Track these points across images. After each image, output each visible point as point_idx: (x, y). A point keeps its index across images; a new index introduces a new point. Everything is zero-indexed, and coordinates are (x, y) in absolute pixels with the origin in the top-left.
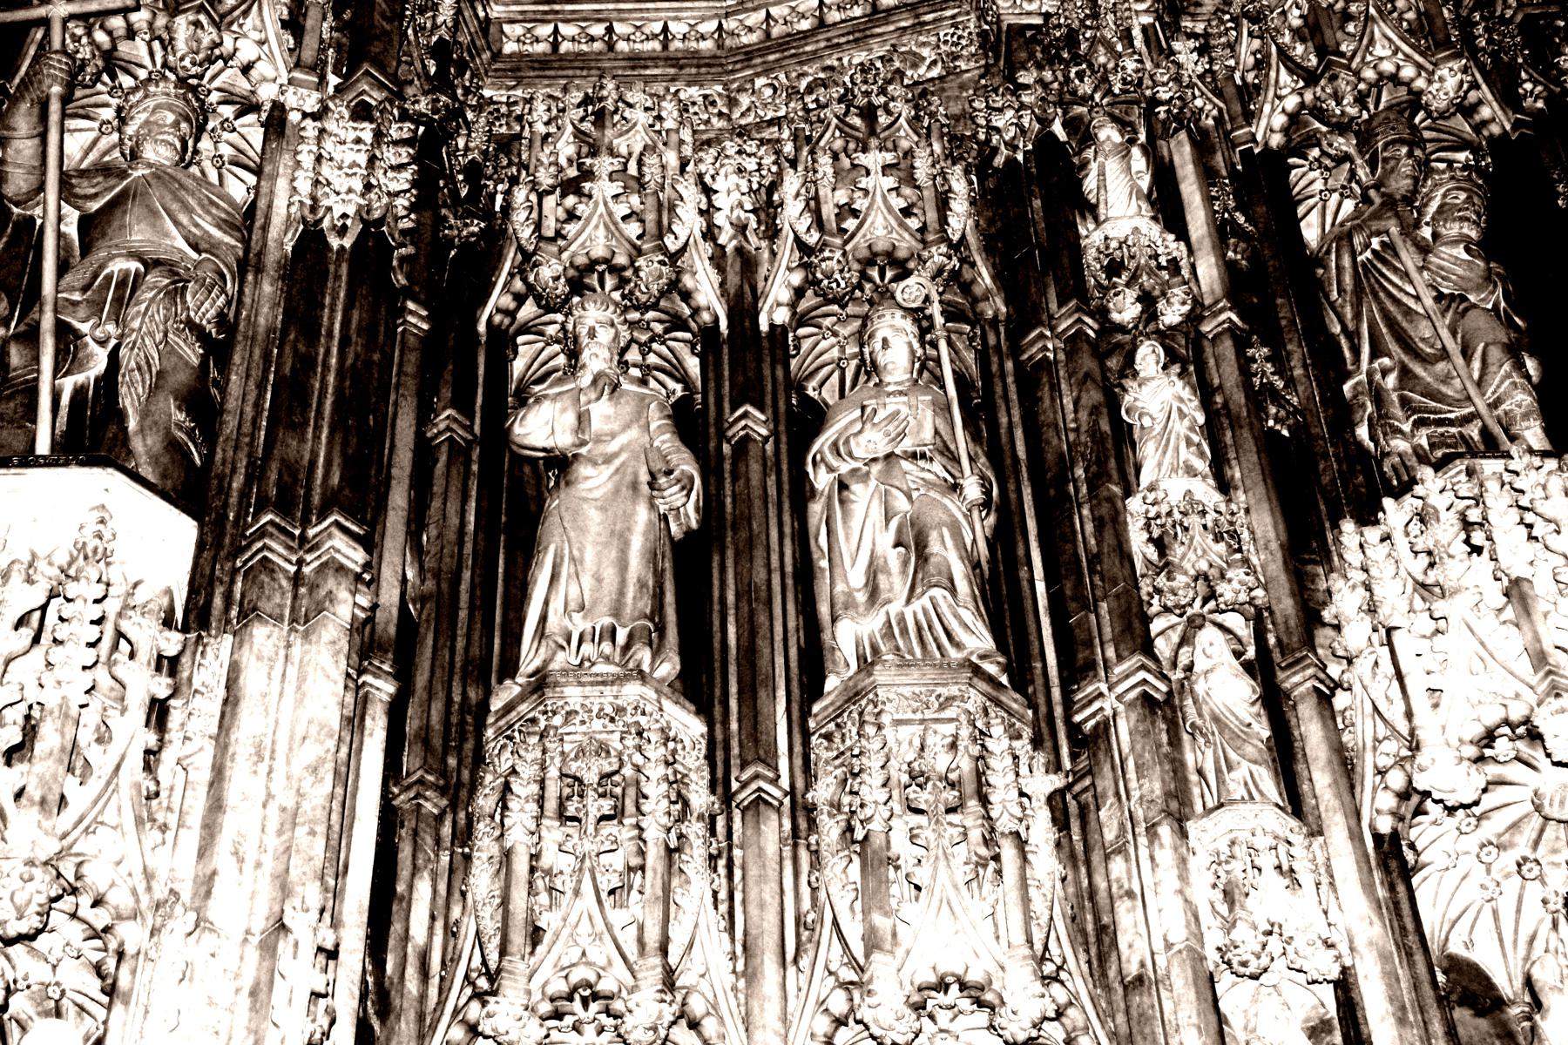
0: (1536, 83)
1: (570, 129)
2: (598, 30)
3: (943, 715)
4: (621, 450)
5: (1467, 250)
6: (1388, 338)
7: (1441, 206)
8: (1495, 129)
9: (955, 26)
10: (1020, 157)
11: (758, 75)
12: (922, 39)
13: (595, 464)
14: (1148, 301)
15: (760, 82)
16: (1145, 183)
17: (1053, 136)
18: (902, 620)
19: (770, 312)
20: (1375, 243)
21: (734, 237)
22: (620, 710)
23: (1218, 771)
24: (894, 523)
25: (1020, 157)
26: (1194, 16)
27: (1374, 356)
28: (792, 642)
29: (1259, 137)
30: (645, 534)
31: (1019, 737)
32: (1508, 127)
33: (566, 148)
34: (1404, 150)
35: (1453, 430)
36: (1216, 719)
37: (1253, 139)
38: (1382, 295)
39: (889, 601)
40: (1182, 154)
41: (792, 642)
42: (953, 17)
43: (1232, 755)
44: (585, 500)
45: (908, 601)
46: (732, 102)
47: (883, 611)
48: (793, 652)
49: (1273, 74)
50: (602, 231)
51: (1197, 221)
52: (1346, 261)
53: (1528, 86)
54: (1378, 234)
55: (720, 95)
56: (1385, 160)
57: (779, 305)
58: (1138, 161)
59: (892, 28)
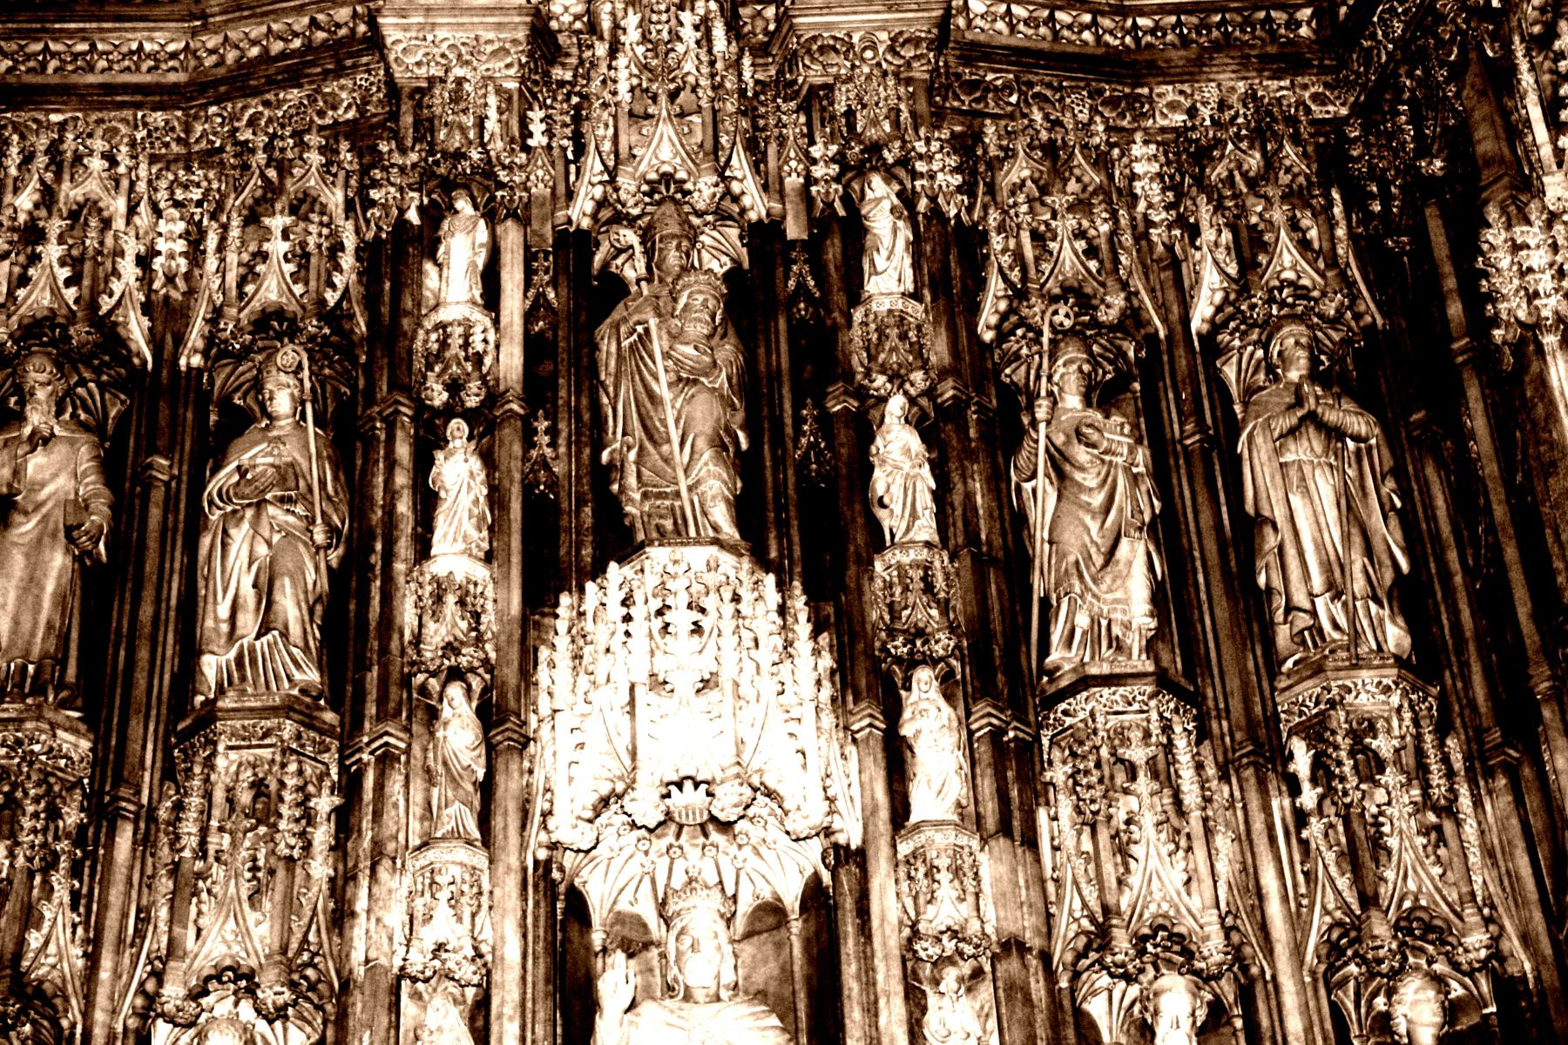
0: (800, 161)
1: (36, 177)
2: (82, 47)
3: (266, 741)
4: (48, 498)
5: (696, 348)
6: (635, 416)
7: (686, 305)
8: (753, 216)
9: (369, 71)
10: (384, 236)
11: (211, 104)
12: (343, 81)
13: (26, 513)
14: (454, 387)
15: (213, 109)
16: (481, 261)
17: (408, 222)
18: (252, 650)
19: (189, 358)
20: (640, 329)
21: (164, 286)
22: (19, 742)
23: (439, 807)
24: (254, 568)
25: (384, 236)
26: (563, 65)
27: (624, 434)
28: (168, 667)
29: (574, 218)
30: (60, 577)
31: (328, 750)
32: (764, 213)
33: (25, 201)
34: (675, 243)
35: (667, 503)
36: (445, 763)
37: (570, 221)
38: (637, 377)
39: (243, 637)
40: (512, 237)
41: (168, 667)
42: (367, 64)
43: (450, 794)
44: (16, 544)
45: (258, 637)
46: (188, 129)
47: (237, 645)
48: (167, 677)
49: (590, 160)
50: (48, 295)
51: (513, 302)
52: (613, 349)
53: (793, 164)
54: (639, 323)
55: (178, 118)
56: (661, 250)
57: (196, 351)
58: (482, 233)
59: (319, 70)
